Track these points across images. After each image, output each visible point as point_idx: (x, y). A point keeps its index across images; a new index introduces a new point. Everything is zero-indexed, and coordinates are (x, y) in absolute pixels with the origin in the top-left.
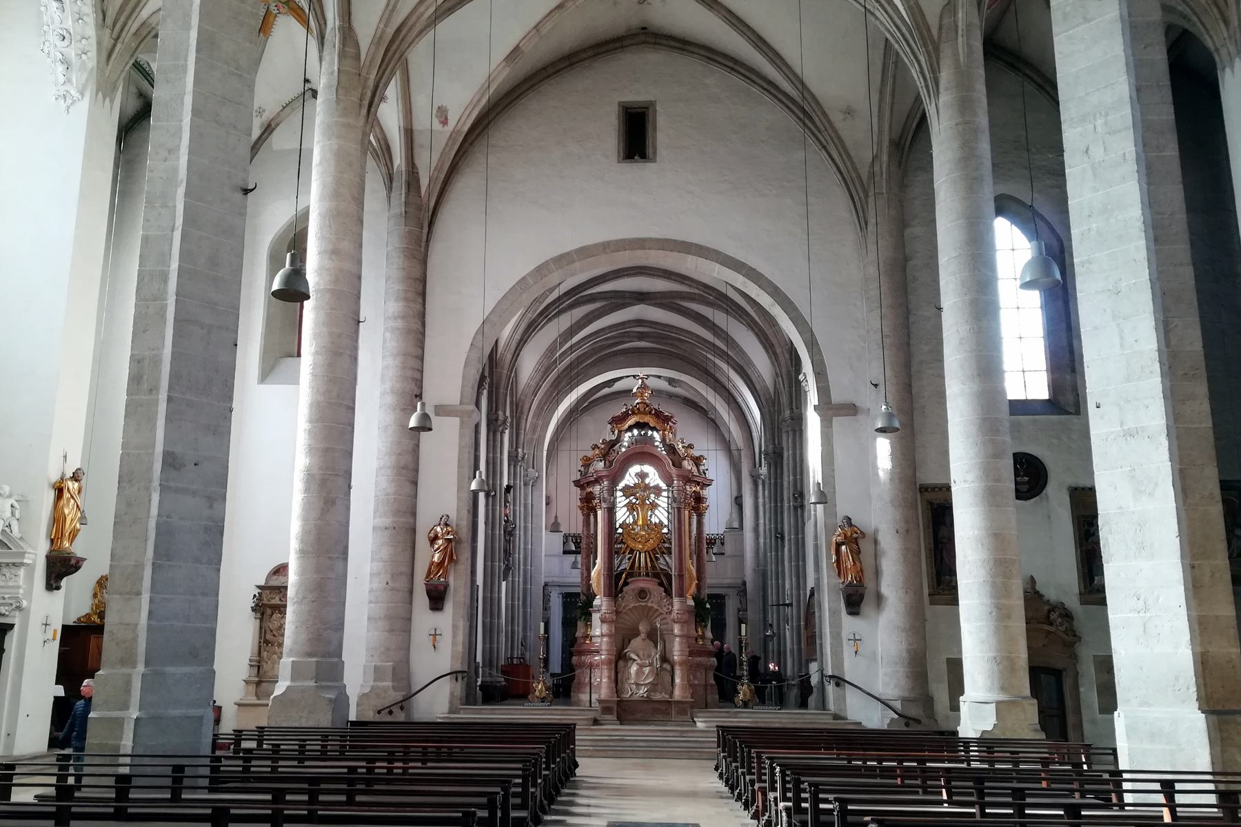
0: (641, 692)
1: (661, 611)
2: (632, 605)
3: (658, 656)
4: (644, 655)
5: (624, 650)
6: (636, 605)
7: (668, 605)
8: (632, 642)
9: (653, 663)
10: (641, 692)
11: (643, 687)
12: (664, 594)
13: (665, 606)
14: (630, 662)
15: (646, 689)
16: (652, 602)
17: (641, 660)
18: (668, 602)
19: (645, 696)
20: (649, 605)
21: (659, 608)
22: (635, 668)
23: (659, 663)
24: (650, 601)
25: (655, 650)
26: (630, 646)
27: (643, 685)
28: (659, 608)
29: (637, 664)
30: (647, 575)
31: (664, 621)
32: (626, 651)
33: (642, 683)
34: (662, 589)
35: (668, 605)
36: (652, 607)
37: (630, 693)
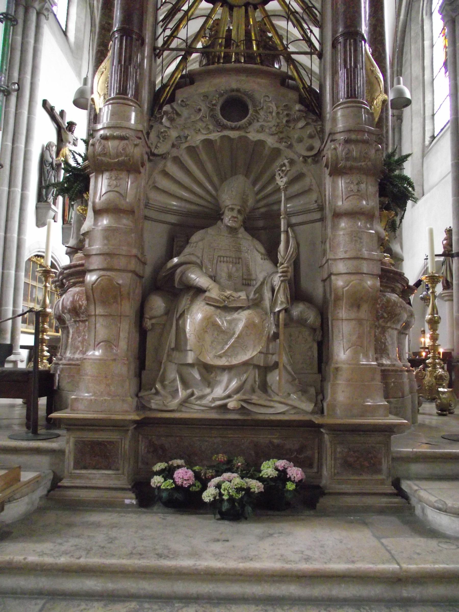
0: (219, 391)
1: (291, 155)
2: (201, 137)
3: (277, 280)
4: (230, 276)
5: (171, 257)
6: (215, 136)
7: (311, 137)
8: (195, 238)
9: (261, 299)
10: (219, 391)
11: (225, 378)
12: (298, 107)
13: (300, 140)
14: (184, 302)
15: (234, 384)
16: (262, 130)
17: (222, 288)
18: (309, 130)
19: (232, 404)
20: (253, 136)
21: (282, 146)
22: (199, 316)
23: (281, 297)
24: (256, 125)
25: (268, 265)
26: (187, 250)
27: (224, 369)
28: (282, 146)
29: (210, 302)
30: (250, 58)
31: (296, 188)
32: (176, 260)
33: (223, 362)
34: (293, 95)
35: (311, 137)
36: (261, 143)
37: (182, 394)
